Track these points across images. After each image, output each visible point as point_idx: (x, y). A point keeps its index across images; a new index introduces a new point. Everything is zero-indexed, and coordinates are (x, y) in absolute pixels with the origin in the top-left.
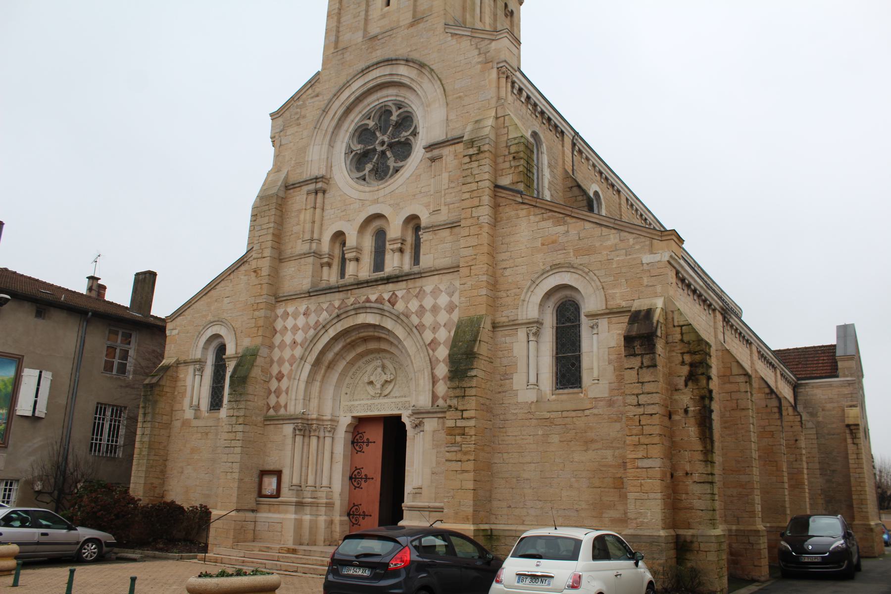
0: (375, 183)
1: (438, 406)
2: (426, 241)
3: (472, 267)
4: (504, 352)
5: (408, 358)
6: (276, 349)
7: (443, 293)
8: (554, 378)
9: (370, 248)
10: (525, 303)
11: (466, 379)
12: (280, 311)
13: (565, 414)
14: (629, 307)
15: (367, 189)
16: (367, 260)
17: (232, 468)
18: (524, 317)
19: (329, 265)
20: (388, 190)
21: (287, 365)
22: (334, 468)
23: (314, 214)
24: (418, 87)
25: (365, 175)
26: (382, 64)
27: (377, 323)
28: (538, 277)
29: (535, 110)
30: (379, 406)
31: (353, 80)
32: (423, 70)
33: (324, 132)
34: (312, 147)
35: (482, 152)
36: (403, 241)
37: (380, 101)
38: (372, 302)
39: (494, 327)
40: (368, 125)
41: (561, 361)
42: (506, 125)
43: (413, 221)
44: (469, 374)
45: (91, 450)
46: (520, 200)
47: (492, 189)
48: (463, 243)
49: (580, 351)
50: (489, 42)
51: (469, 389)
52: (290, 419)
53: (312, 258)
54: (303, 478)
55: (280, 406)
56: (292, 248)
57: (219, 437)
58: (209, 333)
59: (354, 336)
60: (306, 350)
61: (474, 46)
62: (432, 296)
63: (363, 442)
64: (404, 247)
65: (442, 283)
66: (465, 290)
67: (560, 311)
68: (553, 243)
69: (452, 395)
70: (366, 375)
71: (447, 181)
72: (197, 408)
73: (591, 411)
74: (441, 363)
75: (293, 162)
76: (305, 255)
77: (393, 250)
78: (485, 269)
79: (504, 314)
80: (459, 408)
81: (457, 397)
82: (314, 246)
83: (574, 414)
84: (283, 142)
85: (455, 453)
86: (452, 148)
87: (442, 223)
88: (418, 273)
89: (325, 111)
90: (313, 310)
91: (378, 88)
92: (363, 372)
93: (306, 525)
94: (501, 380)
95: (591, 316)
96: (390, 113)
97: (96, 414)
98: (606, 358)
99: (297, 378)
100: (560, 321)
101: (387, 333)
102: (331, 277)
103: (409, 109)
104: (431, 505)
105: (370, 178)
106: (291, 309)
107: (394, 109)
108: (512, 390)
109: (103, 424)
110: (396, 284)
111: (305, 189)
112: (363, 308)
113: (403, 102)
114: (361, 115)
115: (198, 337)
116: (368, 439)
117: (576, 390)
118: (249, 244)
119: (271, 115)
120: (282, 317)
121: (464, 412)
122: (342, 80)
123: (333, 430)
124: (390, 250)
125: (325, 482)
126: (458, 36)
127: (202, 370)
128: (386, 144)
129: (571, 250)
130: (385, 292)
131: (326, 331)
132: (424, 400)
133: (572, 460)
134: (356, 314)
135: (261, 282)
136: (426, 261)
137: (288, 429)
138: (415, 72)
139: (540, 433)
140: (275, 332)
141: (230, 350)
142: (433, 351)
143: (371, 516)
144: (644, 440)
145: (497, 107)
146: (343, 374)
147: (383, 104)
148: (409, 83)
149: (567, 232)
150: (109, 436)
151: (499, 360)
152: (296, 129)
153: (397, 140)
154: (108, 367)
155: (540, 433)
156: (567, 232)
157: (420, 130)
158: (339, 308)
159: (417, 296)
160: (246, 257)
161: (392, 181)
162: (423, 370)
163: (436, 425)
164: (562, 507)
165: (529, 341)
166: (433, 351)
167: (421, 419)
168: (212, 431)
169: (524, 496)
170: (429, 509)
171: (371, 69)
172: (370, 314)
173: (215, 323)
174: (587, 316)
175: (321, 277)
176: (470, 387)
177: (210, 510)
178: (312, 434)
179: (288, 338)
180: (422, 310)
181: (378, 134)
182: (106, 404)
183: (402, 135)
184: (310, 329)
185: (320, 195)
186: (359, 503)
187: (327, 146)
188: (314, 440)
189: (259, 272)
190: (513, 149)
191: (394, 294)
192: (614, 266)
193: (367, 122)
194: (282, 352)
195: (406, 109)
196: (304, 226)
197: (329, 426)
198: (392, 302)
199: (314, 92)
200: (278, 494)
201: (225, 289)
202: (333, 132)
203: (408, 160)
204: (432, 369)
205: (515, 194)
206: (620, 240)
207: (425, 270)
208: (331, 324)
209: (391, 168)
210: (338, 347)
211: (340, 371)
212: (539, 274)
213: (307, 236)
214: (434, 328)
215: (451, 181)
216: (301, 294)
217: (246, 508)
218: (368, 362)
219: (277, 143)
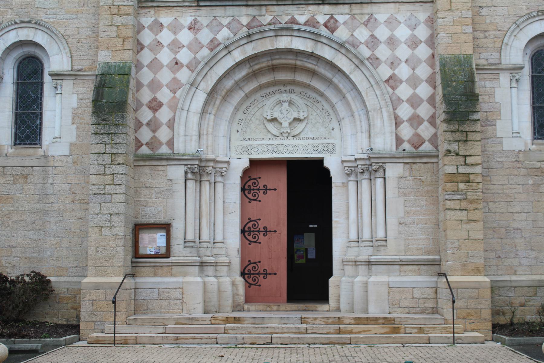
1: (404, 150)
6: (145, 69)
7: (402, 25)
10: (508, 47)
11: (468, 122)
12: (147, 20)
17: (111, 221)
18: (508, 62)
27: (310, 50)
28: (523, 22)
30: (290, 147)
38: (300, 24)
41: (538, 111)
44: (471, 117)
51: (472, 133)
52: (181, 158)
55: (161, 144)
57: (50, 181)
59: (264, 63)
60: (198, 74)
62: (387, 26)
63: (258, 190)
67: (536, 60)
69: (451, 139)
74: (405, 103)
79: (482, 56)
81: (458, 141)
85: (458, 202)
90: (205, 25)
92: (260, 106)
99: (186, 108)
100: (536, 70)
104: (403, 257)
108: (495, 137)
110: (334, 6)
112: (287, 29)
120: (151, 28)
121: (468, 158)
131: (229, 52)
134: (276, 36)
139: (530, 182)
140: (140, 47)
142: (393, 89)
143: (275, 274)
155: (530, 183)
158: (249, 26)
159: (366, 24)
163: (401, 170)
167: (381, 164)
168: (34, 173)
170: (401, 263)
172: (297, 38)
176: (473, 132)
178: (205, 178)
179: (165, 57)
180: (373, 42)
184: (202, 48)
188: (206, 187)
191: (332, 17)
200: (167, 255)
204: (395, 109)
208: (237, 45)
214: (392, 63)
218: (267, 95)
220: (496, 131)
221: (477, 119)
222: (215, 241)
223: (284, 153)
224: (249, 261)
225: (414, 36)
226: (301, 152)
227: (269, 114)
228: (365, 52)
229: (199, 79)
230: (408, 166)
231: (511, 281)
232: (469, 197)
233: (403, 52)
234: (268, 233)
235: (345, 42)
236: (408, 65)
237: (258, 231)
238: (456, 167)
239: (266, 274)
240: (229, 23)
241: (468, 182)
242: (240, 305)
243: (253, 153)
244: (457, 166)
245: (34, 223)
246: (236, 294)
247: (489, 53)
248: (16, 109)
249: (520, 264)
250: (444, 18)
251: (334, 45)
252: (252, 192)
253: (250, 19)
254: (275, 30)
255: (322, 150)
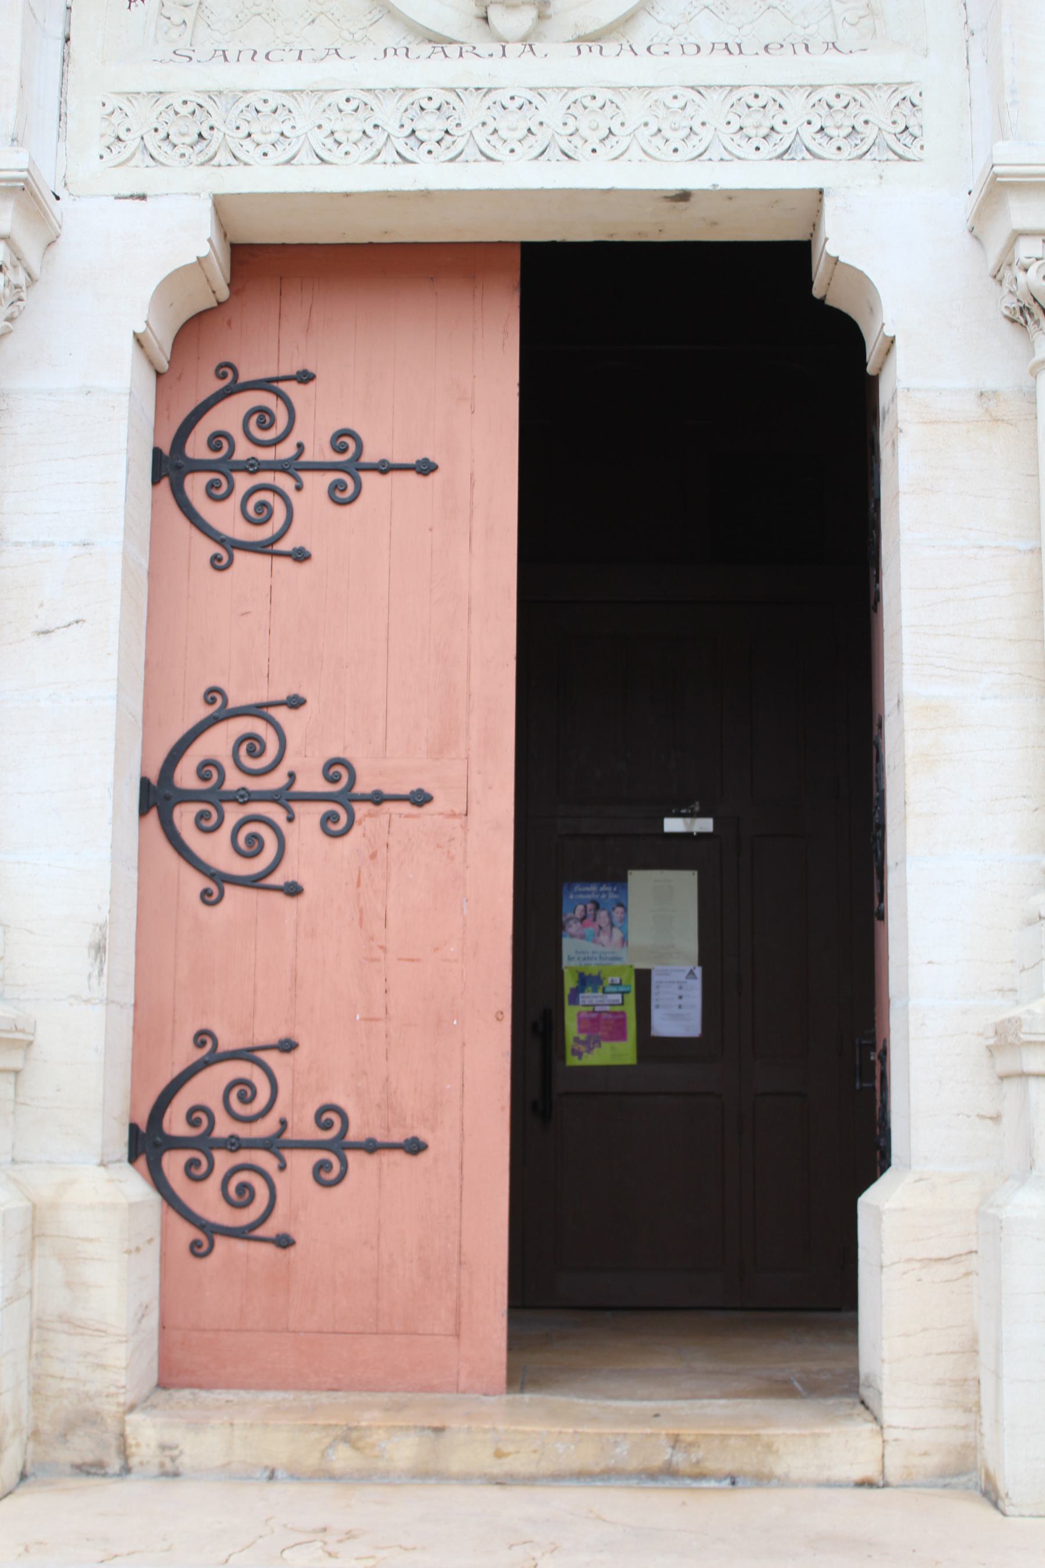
30: (552, 111)
63: (293, 467)
116: (341, 439)
143: (415, 1147)
223: (502, 153)
224: (202, 1037)
226: (635, 153)
234: (361, 809)
239: (340, 1146)
242: (91, 1419)
243: (249, 151)
246: (64, 1319)
252: (243, 482)
255: (808, 132)
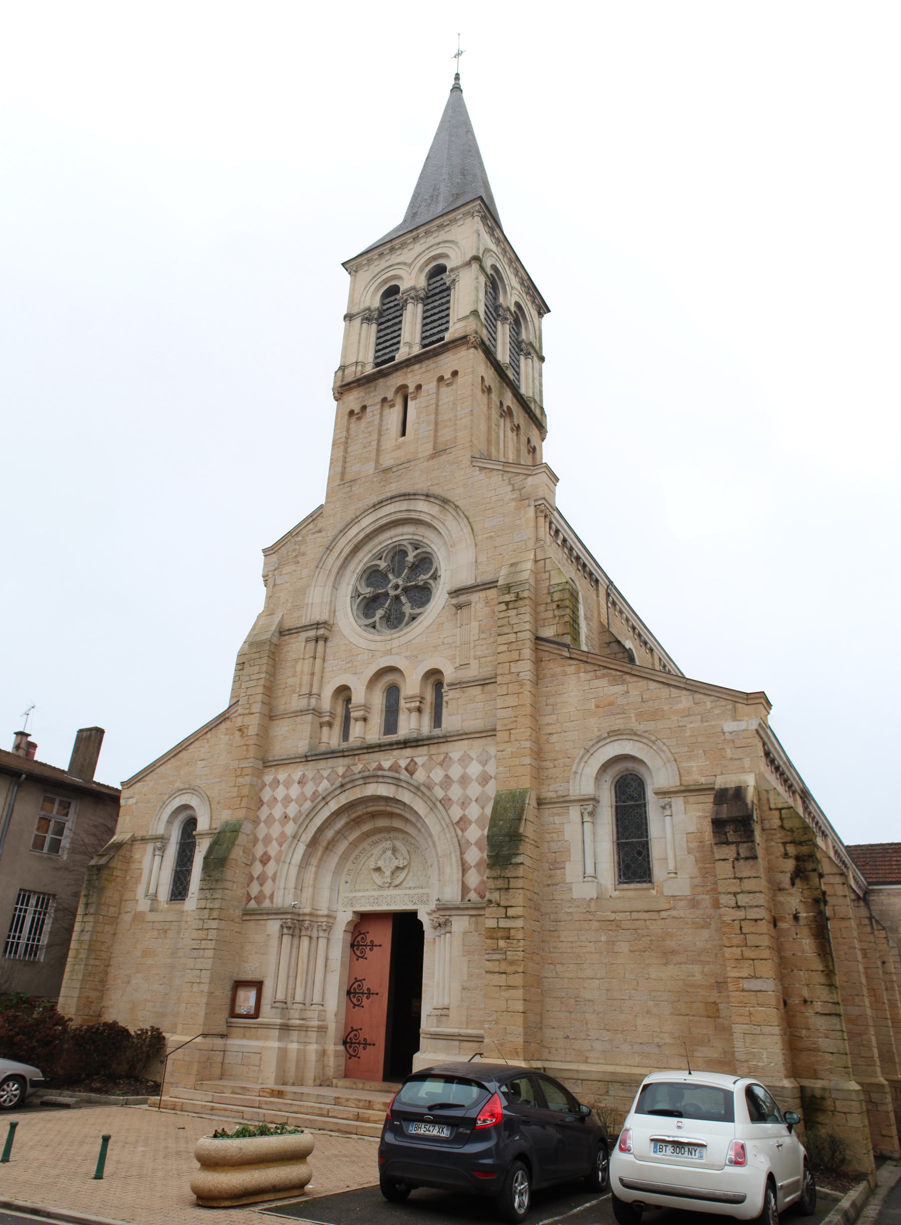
0: (388, 632)
1: (469, 900)
2: (452, 699)
3: (512, 731)
4: (554, 835)
5: (429, 840)
6: (262, 825)
7: (474, 761)
8: (616, 869)
9: (380, 706)
10: (578, 776)
11: (510, 866)
12: (268, 778)
13: (635, 915)
14: (711, 784)
15: (378, 638)
16: (377, 720)
17: (200, 977)
18: (577, 793)
19: (330, 725)
20: (403, 640)
21: (275, 844)
22: (328, 979)
23: (314, 664)
24: (440, 525)
25: (375, 622)
26: (398, 499)
27: (391, 796)
28: (593, 746)
29: (571, 555)
30: (389, 899)
31: (363, 516)
32: (446, 507)
33: (327, 572)
34: (313, 588)
35: (521, 599)
36: (422, 700)
37: (394, 540)
38: (385, 770)
39: (539, 804)
40: (379, 566)
41: (624, 848)
42: (547, 569)
43: (434, 677)
44: (514, 861)
45: (5, 952)
46: (567, 655)
47: (533, 641)
48: (500, 703)
49: (647, 837)
50: (524, 477)
51: (514, 880)
53: (311, 715)
54: (290, 991)
55: (265, 897)
56: (286, 703)
57: (182, 936)
58: (177, 803)
59: (360, 811)
60: (300, 826)
61: (507, 482)
62: (460, 764)
63: (366, 946)
64: (422, 706)
65: (474, 748)
66: (504, 759)
67: (620, 787)
68: (609, 705)
69: (493, 887)
70: (373, 859)
71: (477, 632)
72: (154, 898)
73: (669, 913)
74: (473, 846)
75: (289, 605)
76: (302, 712)
77: (410, 710)
78: (529, 734)
79: (551, 788)
80: (502, 904)
81: (500, 889)
82: (313, 702)
83: (646, 916)
84: (278, 582)
85: (497, 963)
86: (482, 594)
87: (472, 679)
88: (443, 737)
89: (329, 549)
90: (310, 778)
91: (392, 525)
92: (369, 855)
93: (292, 1056)
94: (551, 870)
95: (661, 793)
96: (405, 553)
97: (17, 904)
98: (684, 845)
99: (288, 861)
100: (620, 799)
101: (402, 807)
102: (332, 739)
103: (429, 550)
104: (463, 1031)
105: (381, 626)
106: (282, 776)
107: (410, 549)
108: (564, 882)
109: (24, 917)
110: (415, 749)
111: (304, 635)
112: (373, 776)
113: (422, 541)
114: (370, 555)
115: (161, 807)
117: (644, 885)
118: (232, 697)
119: (264, 551)
120: (271, 785)
121: (509, 909)
122: (350, 516)
123: (329, 929)
124: (405, 709)
125: (317, 999)
126: (487, 470)
127: (163, 849)
128: (401, 588)
129: (633, 715)
130: (402, 758)
131: (327, 803)
132: (452, 894)
133: (647, 976)
134: (365, 784)
135: (248, 743)
136: (451, 722)
137: (274, 926)
138: (437, 508)
139: (604, 938)
140: (261, 803)
141: (203, 825)
142: (463, 831)
144: (748, 953)
145: (535, 549)
146: (344, 858)
147: (397, 543)
148: (429, 521)
149: (627, 692)
150: (30, 933)
151: (546, 844)
152: (293, 567)
153: (414, 583)
154: (38, 844)
155: (603, 939)
156: (627, 692)
157: (444, 573)
158: (343, 776)
159: (441, 764)
160: (228, 713)
161: (409, 629)
162: (450, 854)
163: (467, 925)
164: (638, 1040)
165: (583, 823)
166: (463, 831)
167: (447, 917)
168: (172, 928)
169: (586, 1024)
171: (384, 504)
173: (184, 791)
174: (656, 793)
175: (320, 740)
176: (515, 878)
177: (164, 1034)
178: (303, 933)
179: (278, 812)
180: (447, 781)
181: (391, 576)
182: (30, 891)
183: (420, 579)
185: (321, 643)
186: (359, 1028)
187: (331, 588)
188: (305, 942)
189: (245, 730)
190: (556, 597)
191: (412, 760)
192: (687, 735)
193: (378, 562)
194: (269, 828)
195: (424, 550)
196: (301, 678)
197: (325, 923)
198: (411, 771)
199: (315, 527)
200: (256, 1014)
201: (200, 751)
202: (338, 573)
203: (427, 606)
204: (462, 853)
205: (561, 647)
206: (695, 703)
207: (452, 734)
208: (332, 795)
209: (407, 615)
210: (340, 824)
211: (340, 853)
212: (594, 742)
213: (305, 690)
214: (463, 803)
215: (481, 631)
216: (296, 758)
217: (214, 1032)
218: (375, 843)
219: (271, 582)
220: (565, 875)
221: (519, 862)
222: (313, 1003)
224: (352, 1028)
225: (484, 773)
227: (373, 863)
228: (439, 793)
229: (301, 831)
230: (474, 919)
231: (577, 1071)
232: (509, 957)
233: (474, 790)
235: (420, 785)
236: (478, 804)
237: (362, 993)
238: (496, 920)
239: (366, 1044)
240: (329, 775)
241: (509, 938)
244: (498, 918)
245: (164, 977)
247: (558, 785)
248: (176, 867)
249: (592, 1049)
250: (502, 751)
251: (412, 789)
253: (346, 768)
254: (363, 778)
